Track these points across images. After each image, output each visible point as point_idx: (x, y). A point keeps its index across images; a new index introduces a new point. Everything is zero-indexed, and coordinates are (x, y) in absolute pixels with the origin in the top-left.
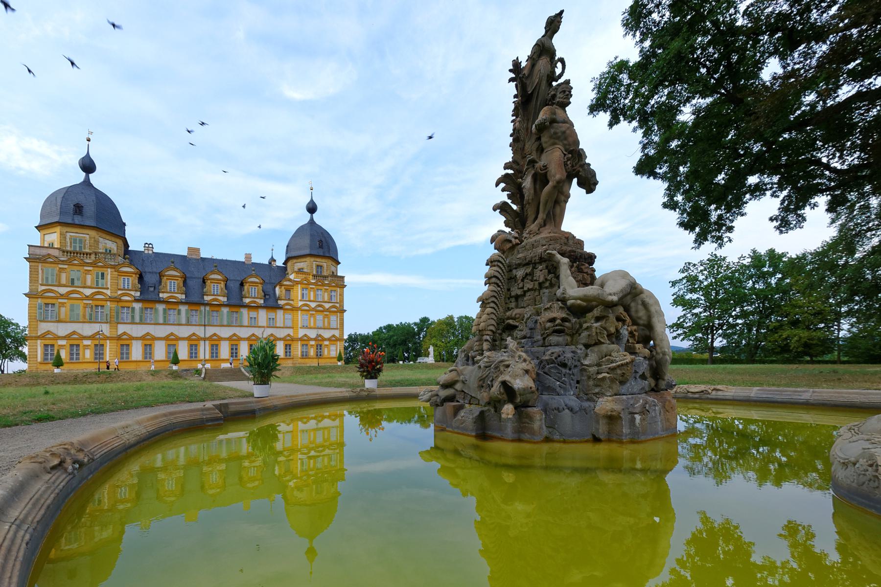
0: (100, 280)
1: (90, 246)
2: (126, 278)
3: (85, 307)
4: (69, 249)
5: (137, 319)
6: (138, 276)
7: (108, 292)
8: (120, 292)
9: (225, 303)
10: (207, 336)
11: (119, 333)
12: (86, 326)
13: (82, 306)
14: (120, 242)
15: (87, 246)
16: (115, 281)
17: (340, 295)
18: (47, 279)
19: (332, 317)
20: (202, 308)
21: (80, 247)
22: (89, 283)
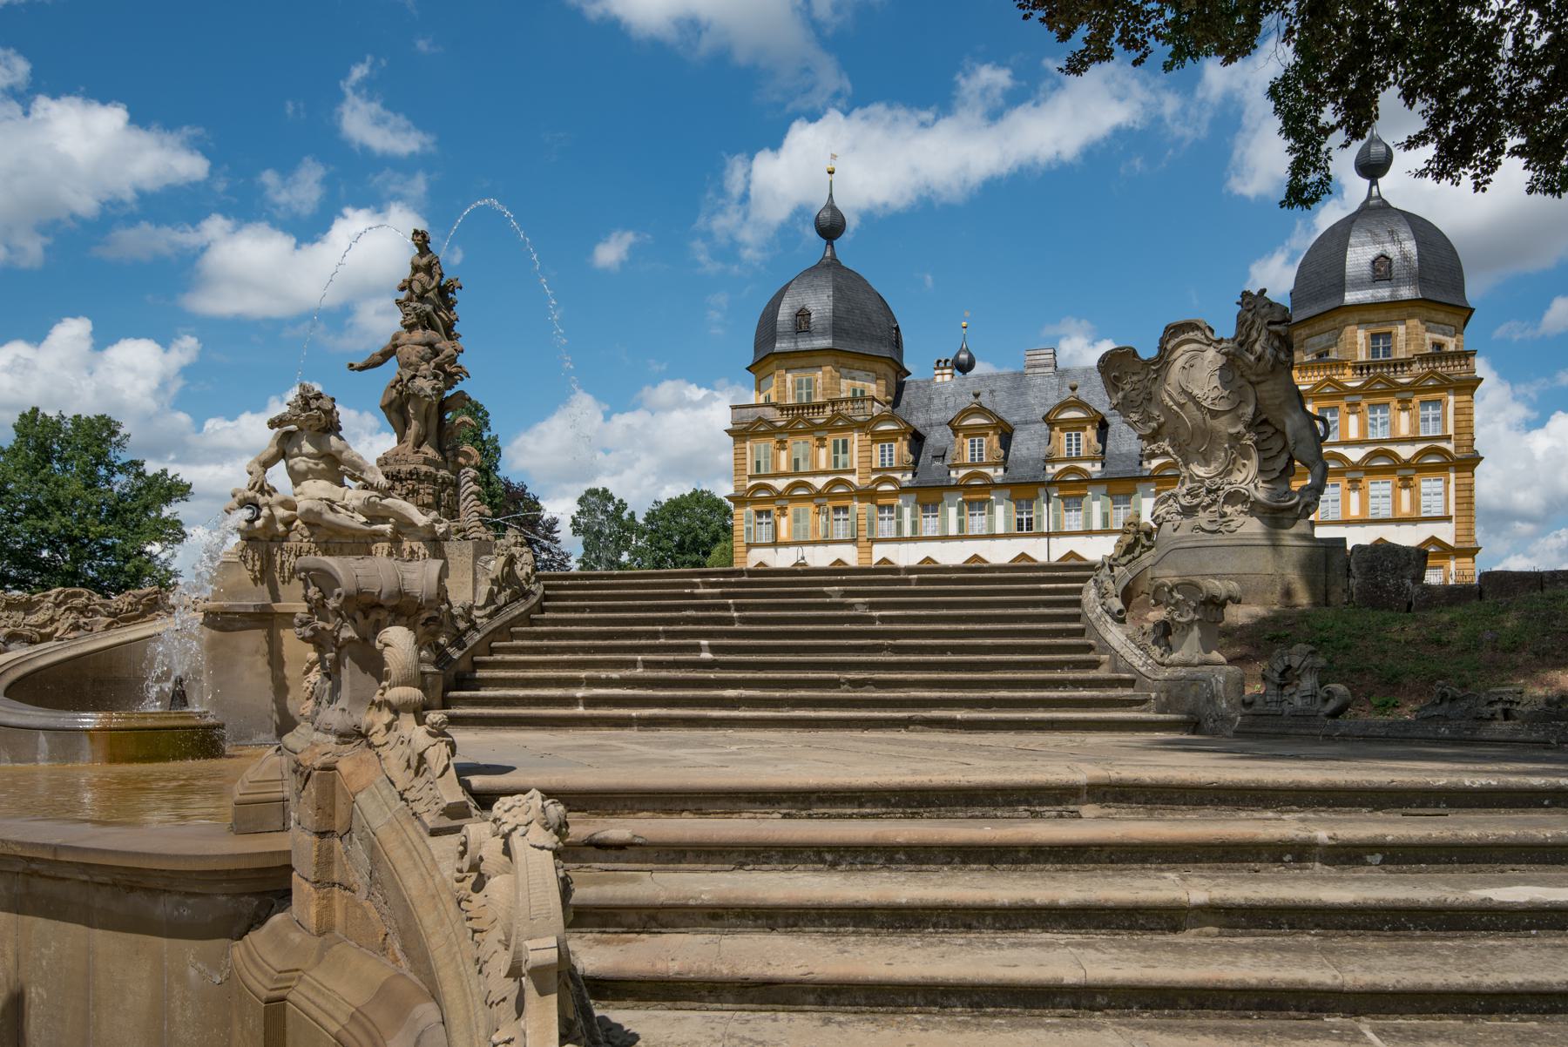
0: (840, 455)
1: (824, 389)
4: (790, 401)
5: (907, 532)
6: (908, 437)
7: (854, 479)
8: (874, 477)
9: (1094, 477)
10: (1054, 558)
11: (875, 560)
12: (820, 549)
16: (864, 454)
17: (1457, 411)
18: (758, 463)
19: (1423, 484)
20: (1041, 491)
21: (809, 395)
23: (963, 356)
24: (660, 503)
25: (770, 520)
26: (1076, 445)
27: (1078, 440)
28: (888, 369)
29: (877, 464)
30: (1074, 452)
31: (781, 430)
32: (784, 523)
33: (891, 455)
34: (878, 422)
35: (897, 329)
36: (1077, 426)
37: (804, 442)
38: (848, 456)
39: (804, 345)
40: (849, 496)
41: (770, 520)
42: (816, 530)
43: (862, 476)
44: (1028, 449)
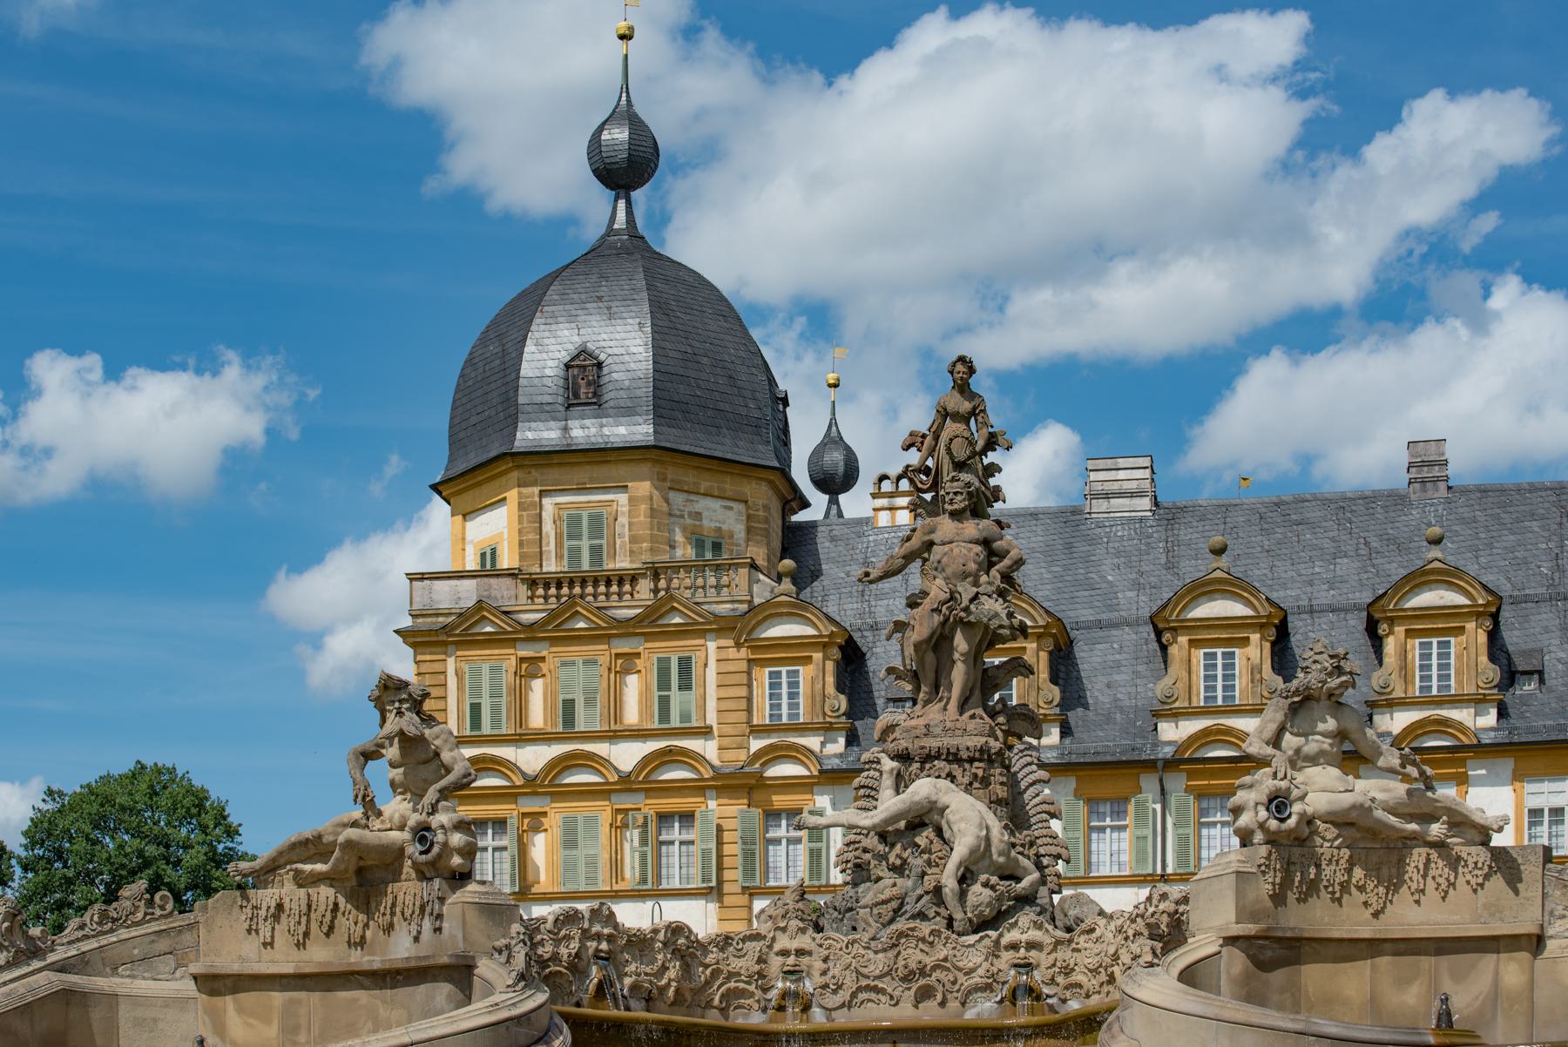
0: (675, 695)
2: (784, 670)
3: (619, 827)
4: (551, 566)
6: (835, 653)
7: (709, 749)
8: (756, 744)
13: (605, 817)
14: (761, 494)
15: (622, 542)
18: (476, 709)
21: (596, 552)
22: (632, 715)
23: (835, 458)
24: (61, 794)
25: (504, 842)
26: (1225, 677)
27: (1229, 666)
28: (770, 493)
29: (762, 716)
30: (1220, 693)
31: (531, 633)
32: (540, 848)
33: (792, 696)
34: (765, 619)
35: (785, 401)
36: (1230, 633)
37: (585, 662)
38: (692, 696)
39: (585, 431)
40: (698, 788)
41: (504, 842)
42: (616, 867)
43: (726, 742)
44: (1109, 686)
